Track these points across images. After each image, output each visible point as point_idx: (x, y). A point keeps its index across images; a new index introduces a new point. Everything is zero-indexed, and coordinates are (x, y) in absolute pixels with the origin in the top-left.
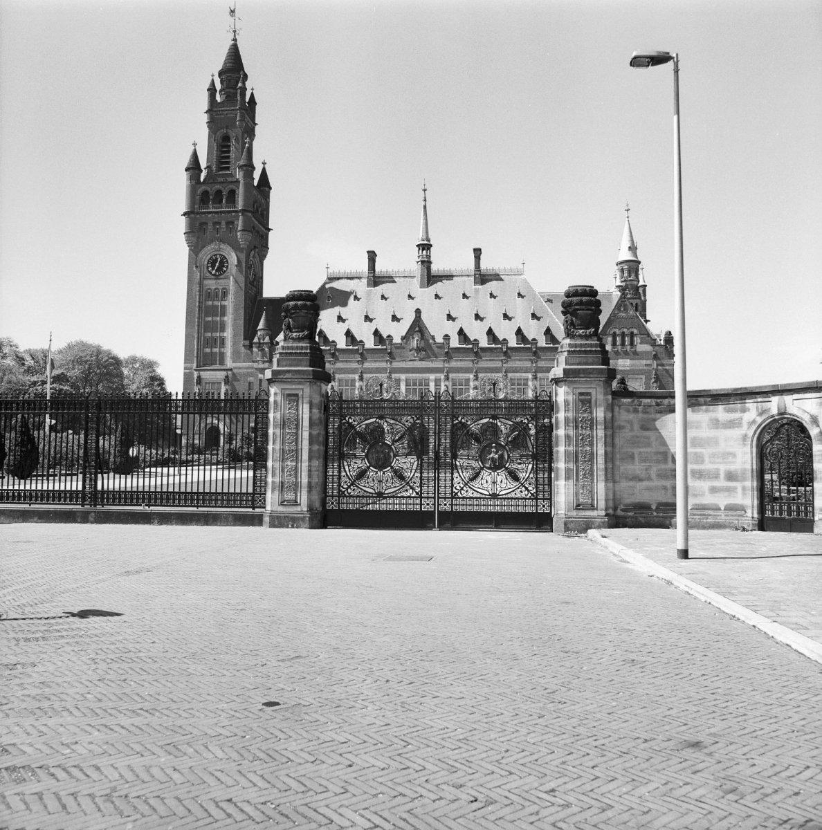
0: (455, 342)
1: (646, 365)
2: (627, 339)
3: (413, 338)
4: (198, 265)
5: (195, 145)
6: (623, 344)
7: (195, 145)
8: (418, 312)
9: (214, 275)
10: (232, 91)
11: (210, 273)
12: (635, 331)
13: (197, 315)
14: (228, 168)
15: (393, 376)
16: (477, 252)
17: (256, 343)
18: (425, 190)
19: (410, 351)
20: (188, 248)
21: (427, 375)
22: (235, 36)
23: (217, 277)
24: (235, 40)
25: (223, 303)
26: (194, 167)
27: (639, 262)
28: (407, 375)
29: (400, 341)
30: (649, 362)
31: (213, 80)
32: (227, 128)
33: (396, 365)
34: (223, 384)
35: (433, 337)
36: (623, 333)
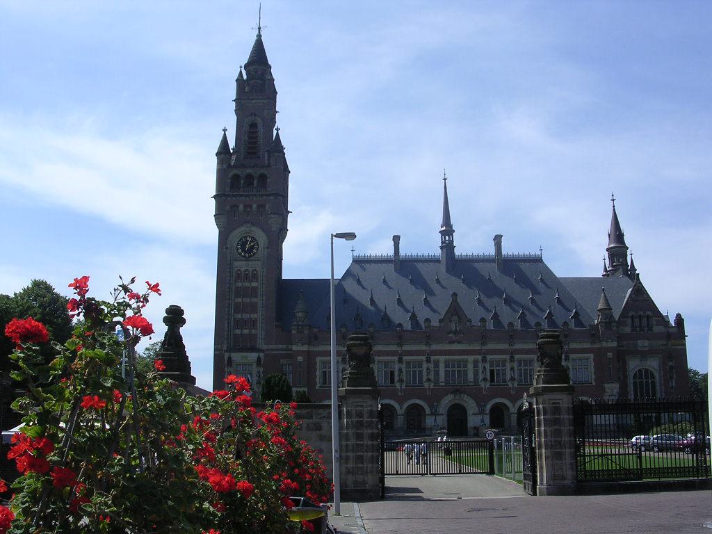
0: (490, 325)
1: (662, 345)
2: (644, 321)
3: (450, 321)
4: (228, 246)
5: (225, 130)
6: (640, 327)
7: (225, 130)
8: (455, 295)
9: (244, 257)
10: (258, 81)
11: (240, 254)
12: (650, 313)
13: (228, 297)
14: (255, 153)
15: (433, 358)
16: (498, 239)
17: (295, 325)
18: (445, 179)
19: (449, 333)
20: (217, 230)
21: (466, 357)
22: (259, 32)
23: (247, 259)
24: (259, 36)
25: (254, 284)
26: (223, 151)
27: (628, 248)
28: (447, 357)
29: (438, 324)
30: (664, 342)
31: (241, 71)
32: (255, 115)
33: (434, 347)
34: (254, 365)
35: (470, 321)
36: (640, 317)
